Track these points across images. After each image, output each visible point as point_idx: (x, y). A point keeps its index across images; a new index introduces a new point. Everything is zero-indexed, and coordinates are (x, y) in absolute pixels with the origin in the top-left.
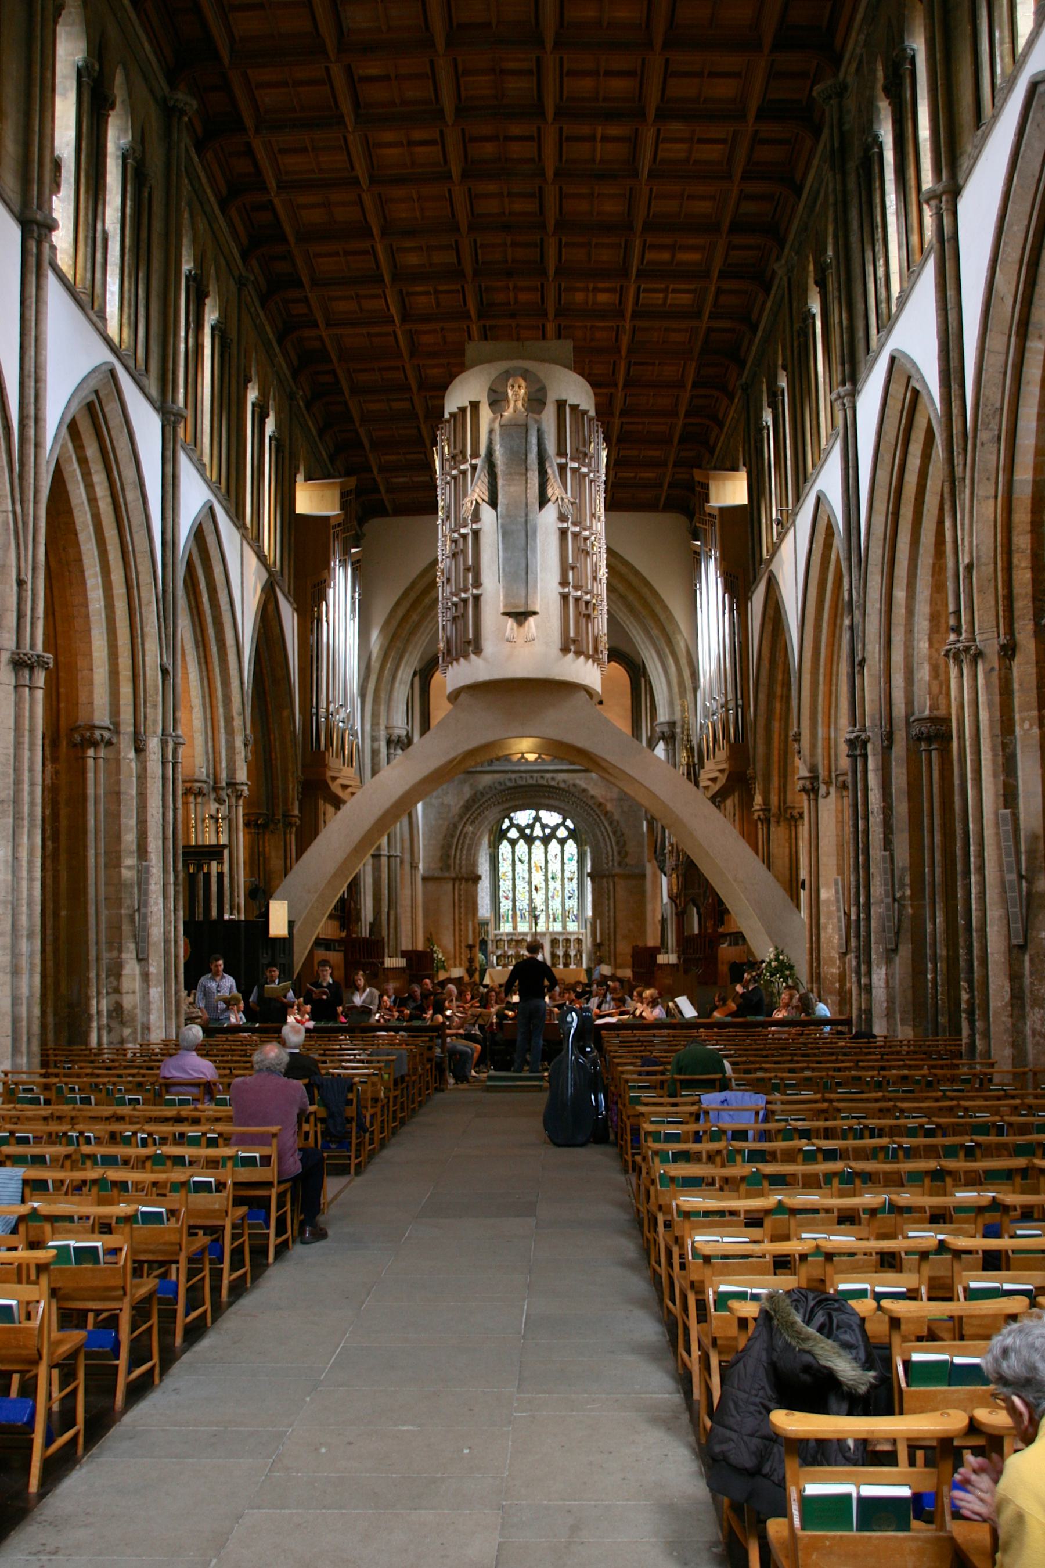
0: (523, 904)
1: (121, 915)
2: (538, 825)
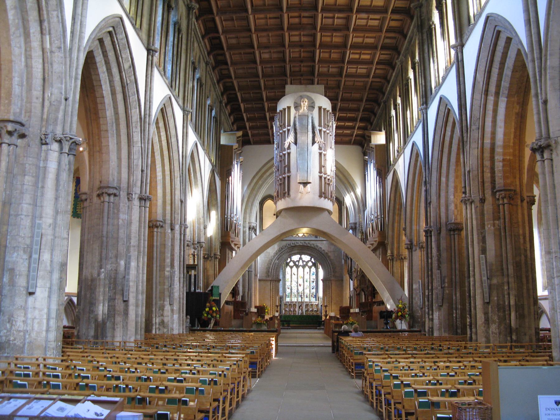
0: (294, 291)
1: (164, 289)
2: (301, 261)
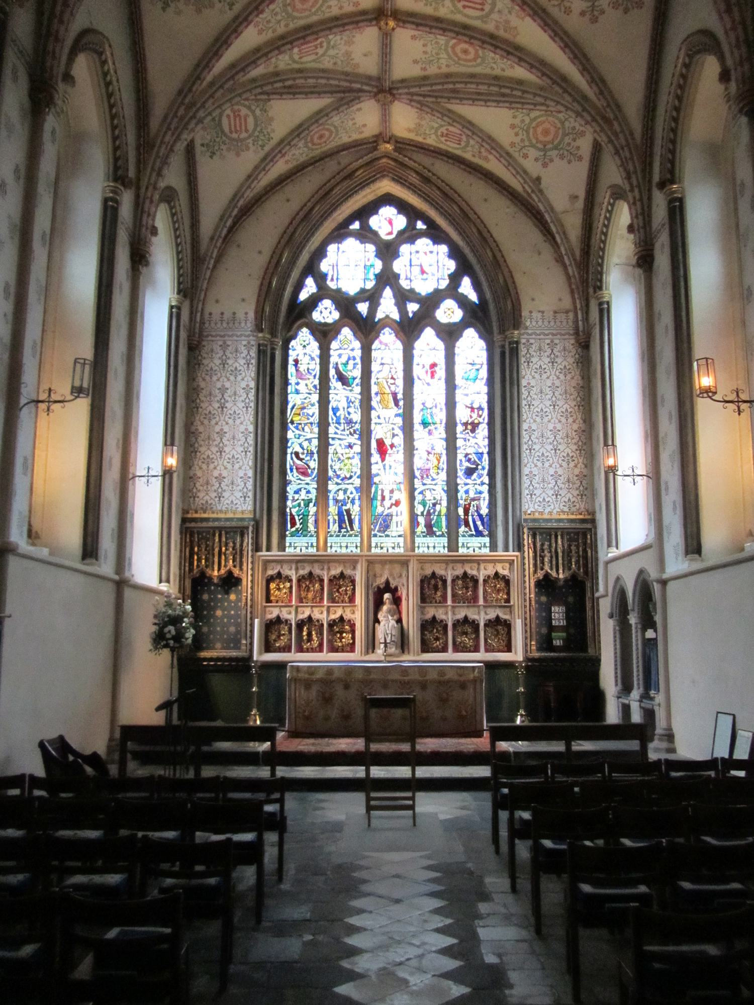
2: (388, 293)
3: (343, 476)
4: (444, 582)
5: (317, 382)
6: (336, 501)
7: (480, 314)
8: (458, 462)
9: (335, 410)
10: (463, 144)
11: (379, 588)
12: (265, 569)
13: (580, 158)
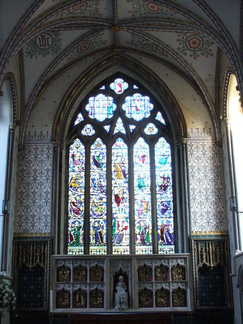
0: (98, 222)
2: (120, 120)
3: (97, 214)
4: (151, 269)
5: (84, 166)
6: (94, 227)
7: (167, 130)
8: (157, 206)
9: (93, 180)
10: (155, 49)
11: (116, 273)
12: (57, 263)
13: (212, 55)
